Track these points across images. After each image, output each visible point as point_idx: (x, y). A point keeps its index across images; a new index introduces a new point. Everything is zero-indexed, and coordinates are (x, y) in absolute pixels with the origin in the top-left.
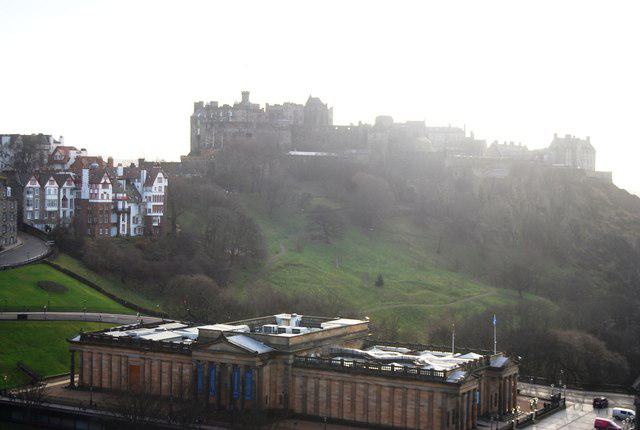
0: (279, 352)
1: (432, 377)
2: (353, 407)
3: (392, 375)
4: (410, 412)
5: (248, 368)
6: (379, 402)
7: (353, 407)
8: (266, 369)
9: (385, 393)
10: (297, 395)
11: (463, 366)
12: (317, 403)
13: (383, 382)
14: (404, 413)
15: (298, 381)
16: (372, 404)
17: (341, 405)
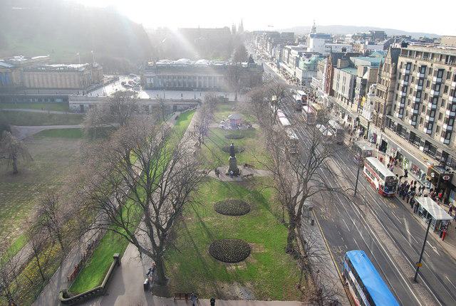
0: (16, 66)
1: (73, 70)
2: (48, 83)
3: (60, 71)
4: (68, 83)
5: (6, 73)
6: (56, 80)
7: (48, 83)
8: (13, 73)
9: (58, 77)
10: (27, 81)
11: (84, 67)
12: (34, 83)
13: (57, 73)
14: (66, 84)
15: (26, 77)
16: (54, 81)
17: (43, 83)
